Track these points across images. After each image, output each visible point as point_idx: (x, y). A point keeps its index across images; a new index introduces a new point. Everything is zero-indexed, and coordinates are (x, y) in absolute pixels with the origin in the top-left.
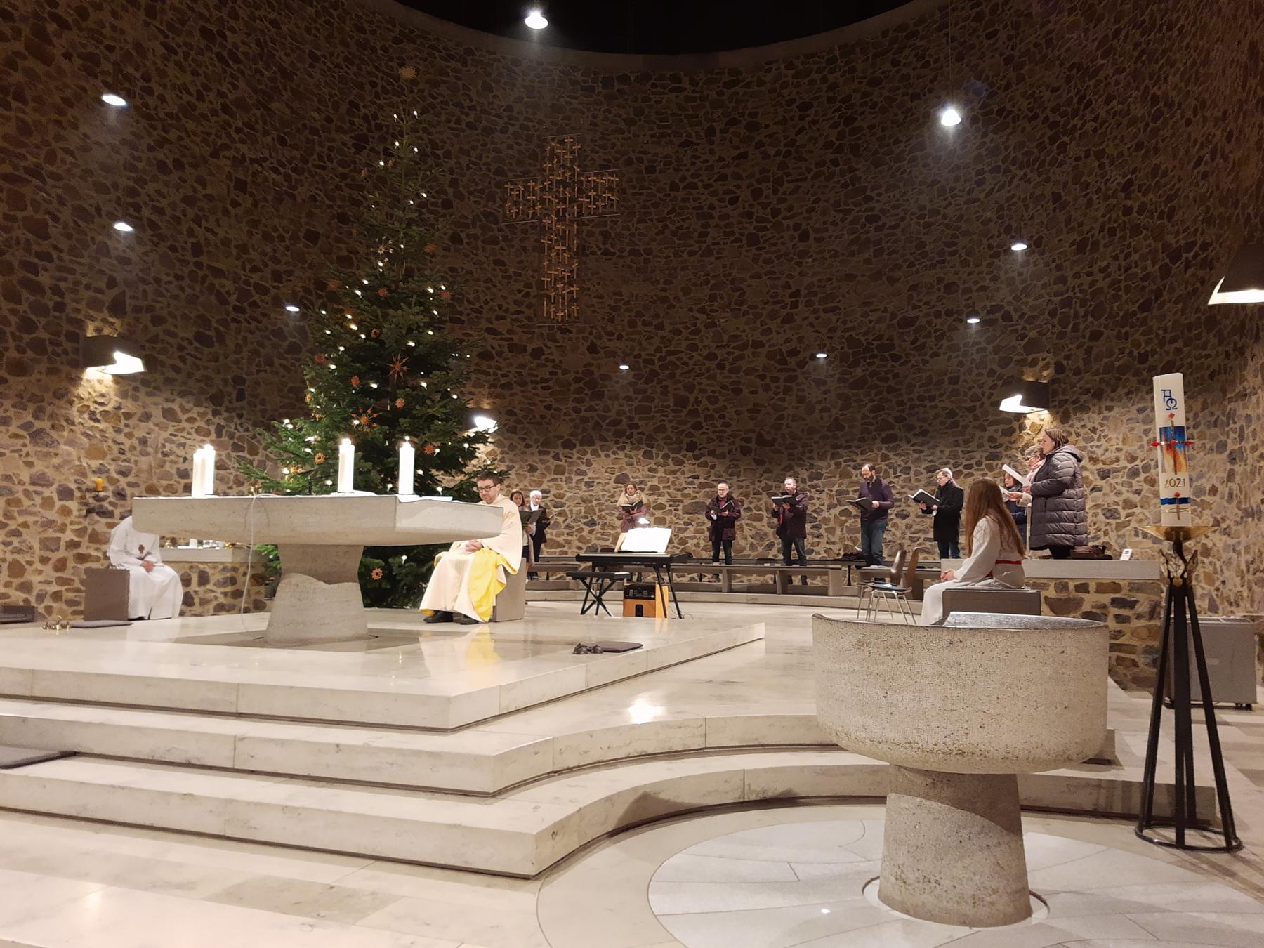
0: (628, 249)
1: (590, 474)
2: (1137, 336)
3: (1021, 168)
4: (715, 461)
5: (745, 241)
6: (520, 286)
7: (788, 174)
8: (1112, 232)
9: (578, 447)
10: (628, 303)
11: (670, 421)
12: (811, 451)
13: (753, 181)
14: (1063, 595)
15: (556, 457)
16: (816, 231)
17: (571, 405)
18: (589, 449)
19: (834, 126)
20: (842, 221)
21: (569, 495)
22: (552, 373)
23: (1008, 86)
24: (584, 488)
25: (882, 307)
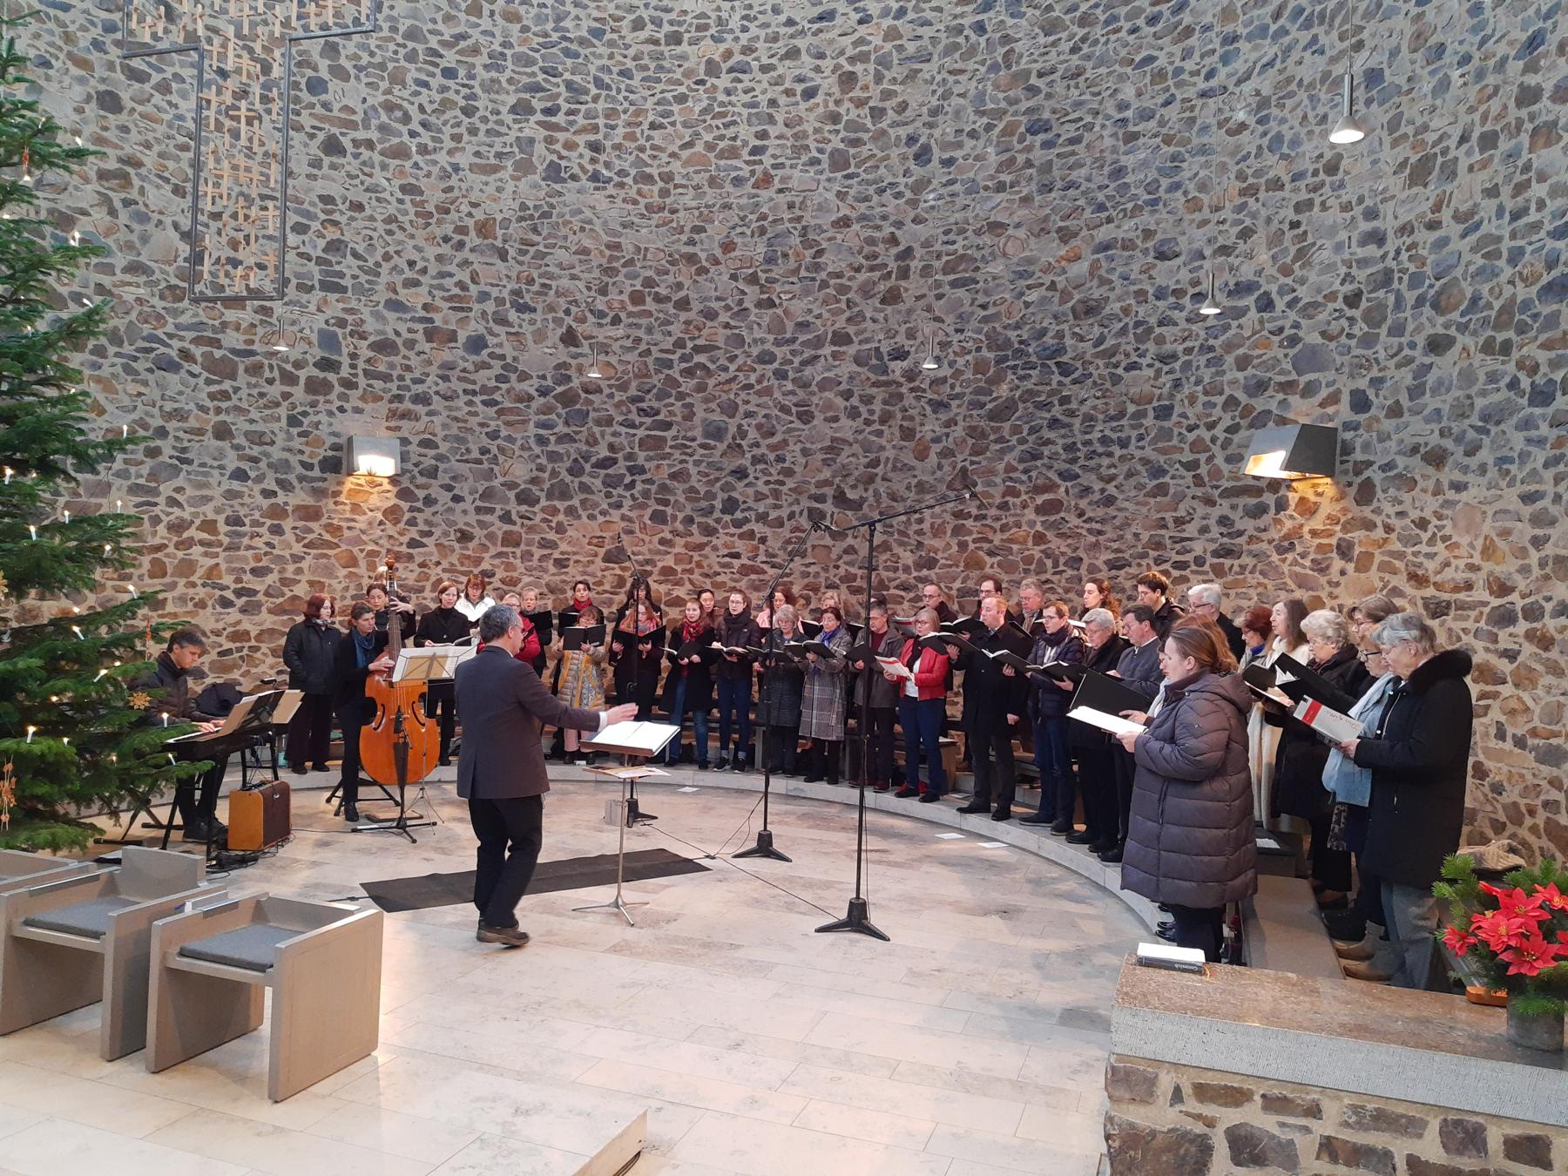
0: (633, 172)
1: (563, 547)
2: (1533, 351)
4: (768, 531)
5: (825, 165)
6: (448, 229)
7: (900, 48)
8: (1489, 141)
9: (544, 502)
10: (630, 262)
11: (697, 463)
12: (920, 521)
13: (842, 61)
14: (1467, 1163)
15: (506, 518)
16: (945, 146)
17: (532, 430)
18: (561, 505)
20: (989, 128)
21: (526, 579)
22: (499, 378)
24: (552, 569)
25: (1047, 280)
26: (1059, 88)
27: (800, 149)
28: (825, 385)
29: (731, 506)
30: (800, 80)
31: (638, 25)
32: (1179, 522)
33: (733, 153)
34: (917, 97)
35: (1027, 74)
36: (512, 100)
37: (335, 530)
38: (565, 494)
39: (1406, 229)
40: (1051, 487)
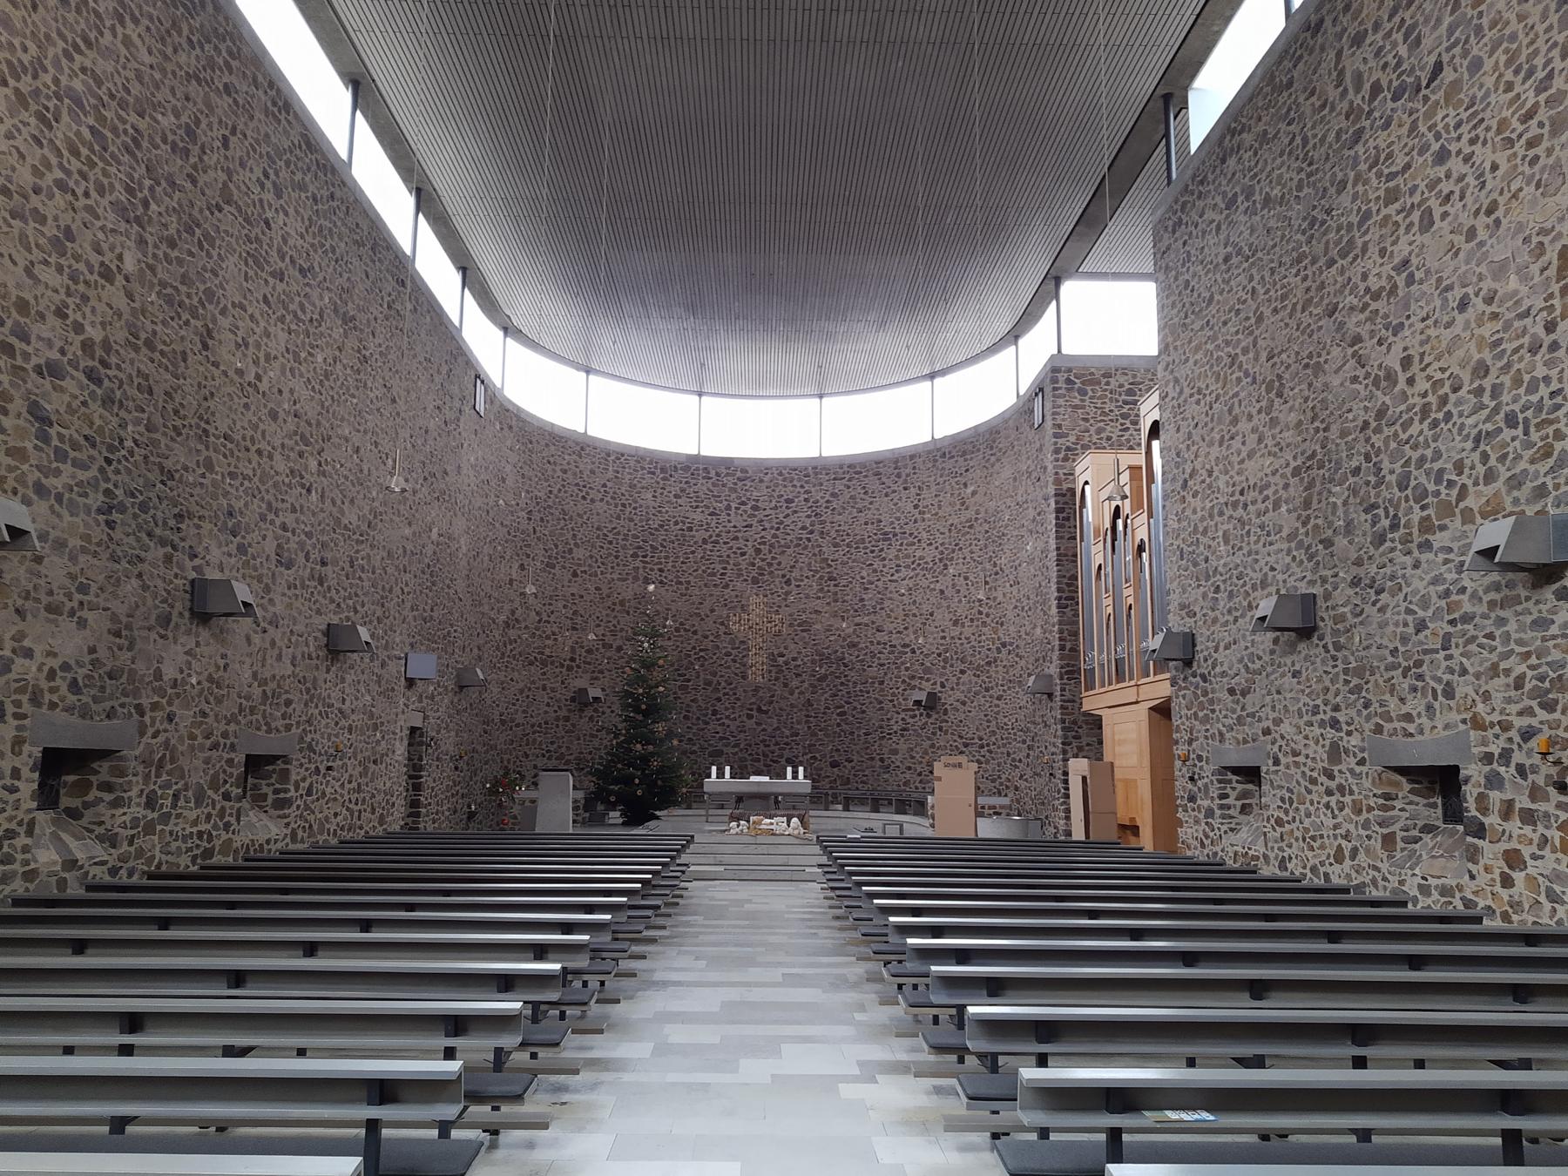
27: (740, 575)
29: (715, 713)
33: (714, 574)
34: (786, 561)
37: (573, 725)
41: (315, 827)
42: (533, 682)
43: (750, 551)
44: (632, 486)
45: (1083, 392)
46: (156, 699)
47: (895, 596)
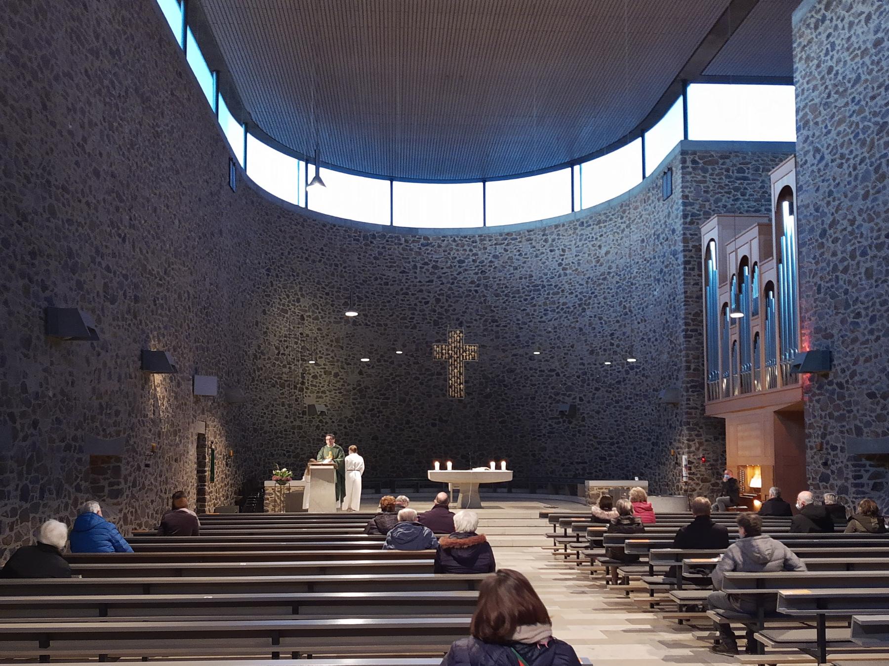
3: (565, 313)
15: (345, 427)
16: (467, 322)
17: (352, 401)
19: (476, 274)
23: (560, 276)
26: (500, 312)
28: (434, 387)
29: (408, 422)
30: (424, 298)
31: (376, 279)
32: (539, 426)
33: (405, 318)
35: (490, 306)
36: (343, 301)
38: (360, 420)
39: (589, 364)
40: (503, 416)
41: (139, 512)
42: (275, 400)
43: (432, 301)
44: (343, 250)
45: (705, 171)
46: (24, 408)
47: (544, 333)
